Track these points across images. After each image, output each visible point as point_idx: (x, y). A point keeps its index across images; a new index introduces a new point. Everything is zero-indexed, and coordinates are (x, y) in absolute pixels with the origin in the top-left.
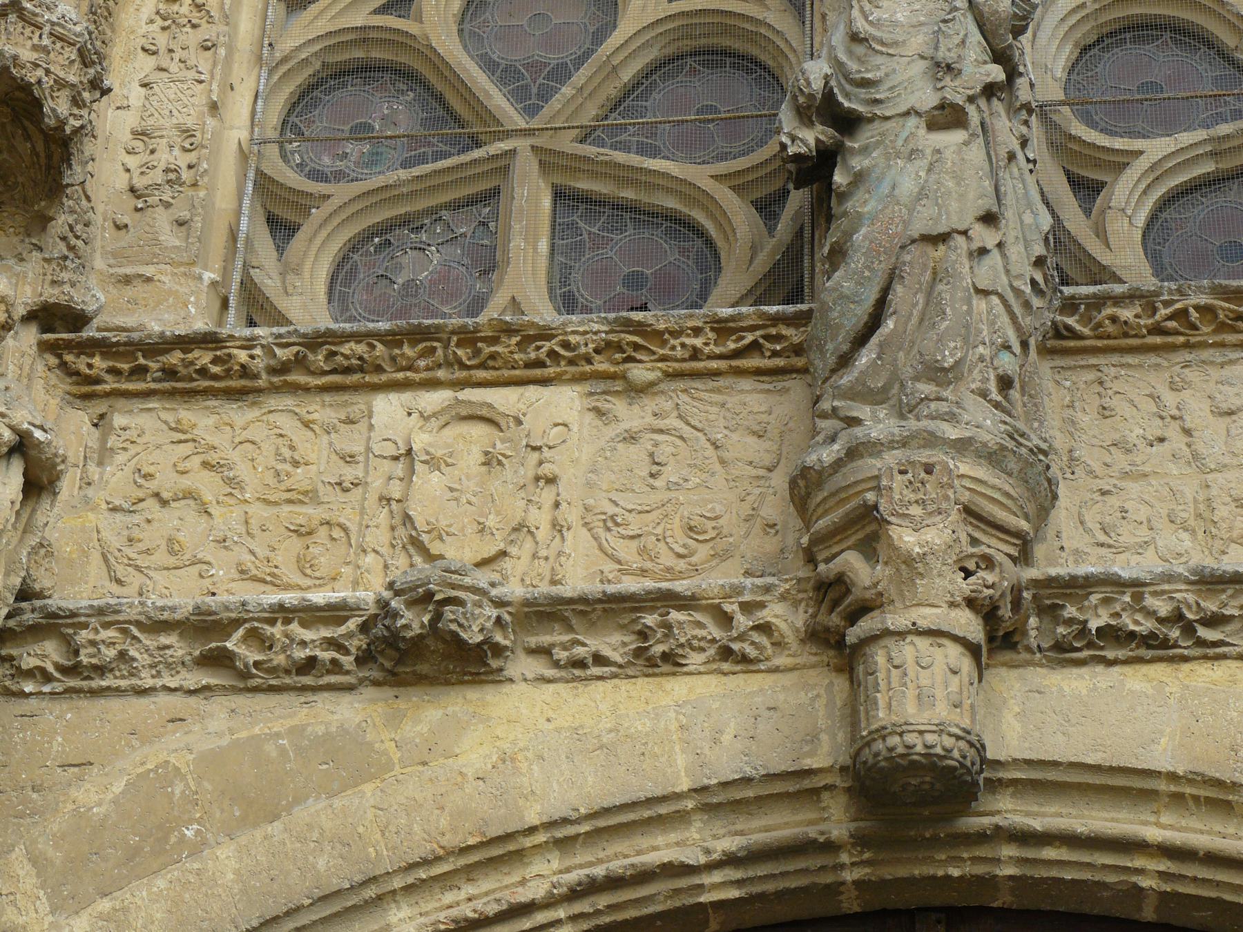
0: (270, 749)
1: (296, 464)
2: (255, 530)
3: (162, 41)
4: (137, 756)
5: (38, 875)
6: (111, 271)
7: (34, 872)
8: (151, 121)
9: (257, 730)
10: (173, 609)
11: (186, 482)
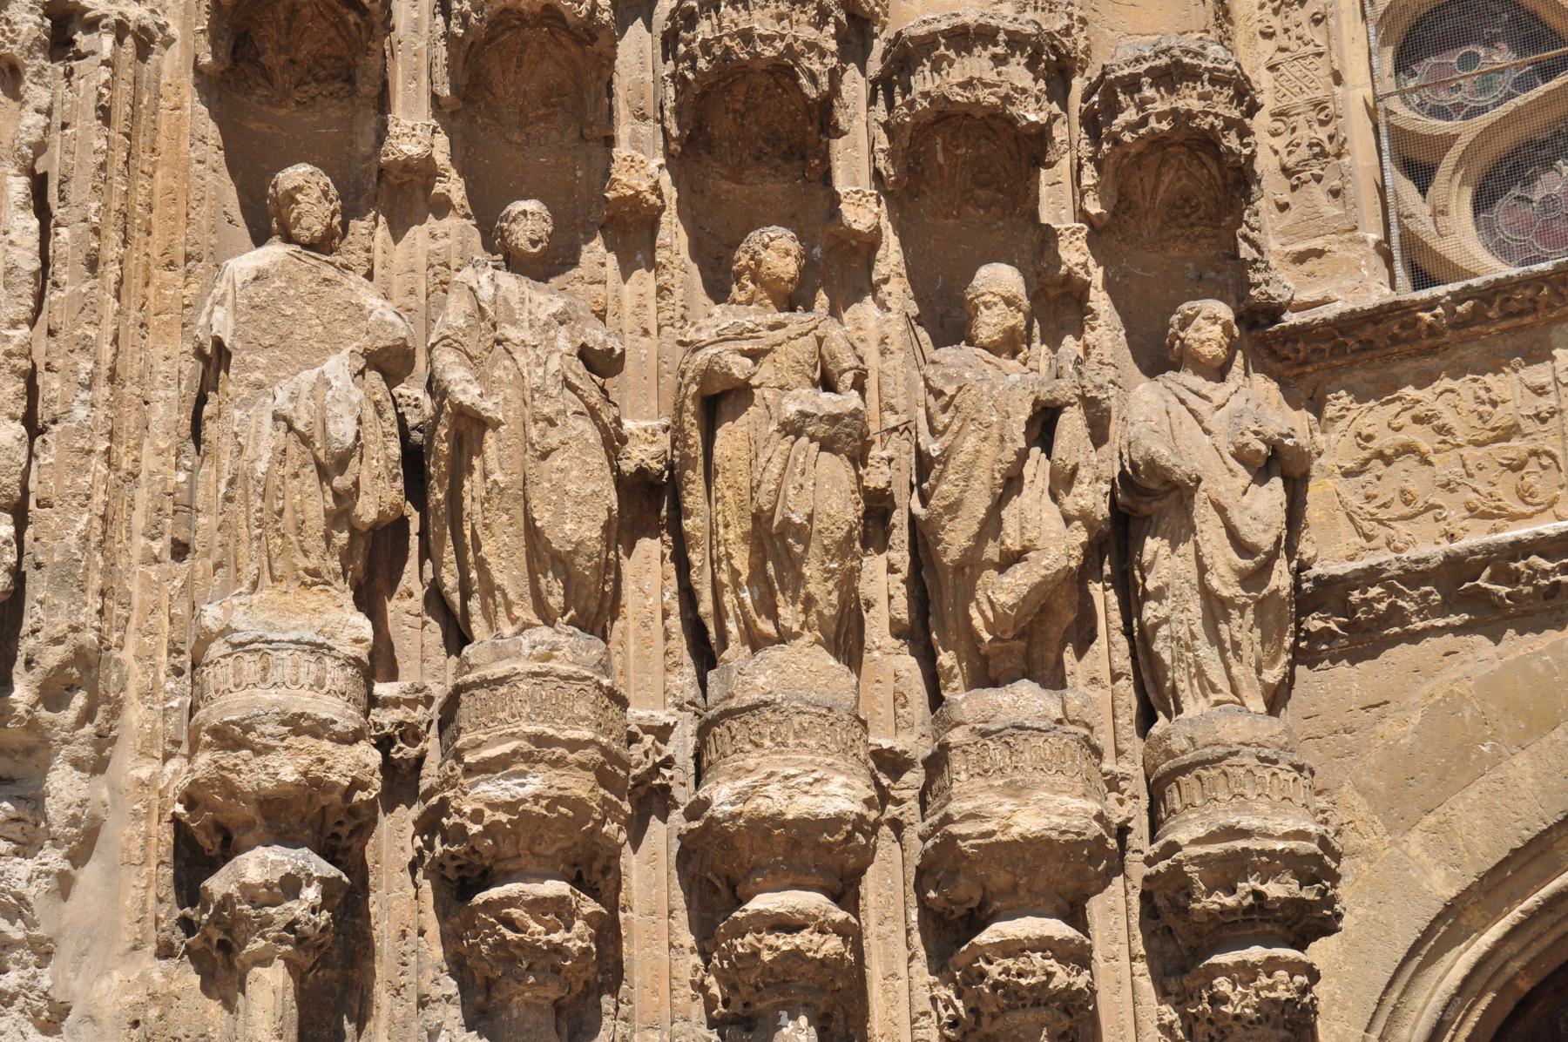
0: (1537, 666)
1: (1494, 404)
2: (1474, 471)
3: (1277, 23)
4: (1425, 689)
5: (1369, 803)
6: (1287, 249)
7: (1364, 801)
8: (1285, 101)
9: (1521, 652)
10: (1426, 560)
11: (1402, 437)
